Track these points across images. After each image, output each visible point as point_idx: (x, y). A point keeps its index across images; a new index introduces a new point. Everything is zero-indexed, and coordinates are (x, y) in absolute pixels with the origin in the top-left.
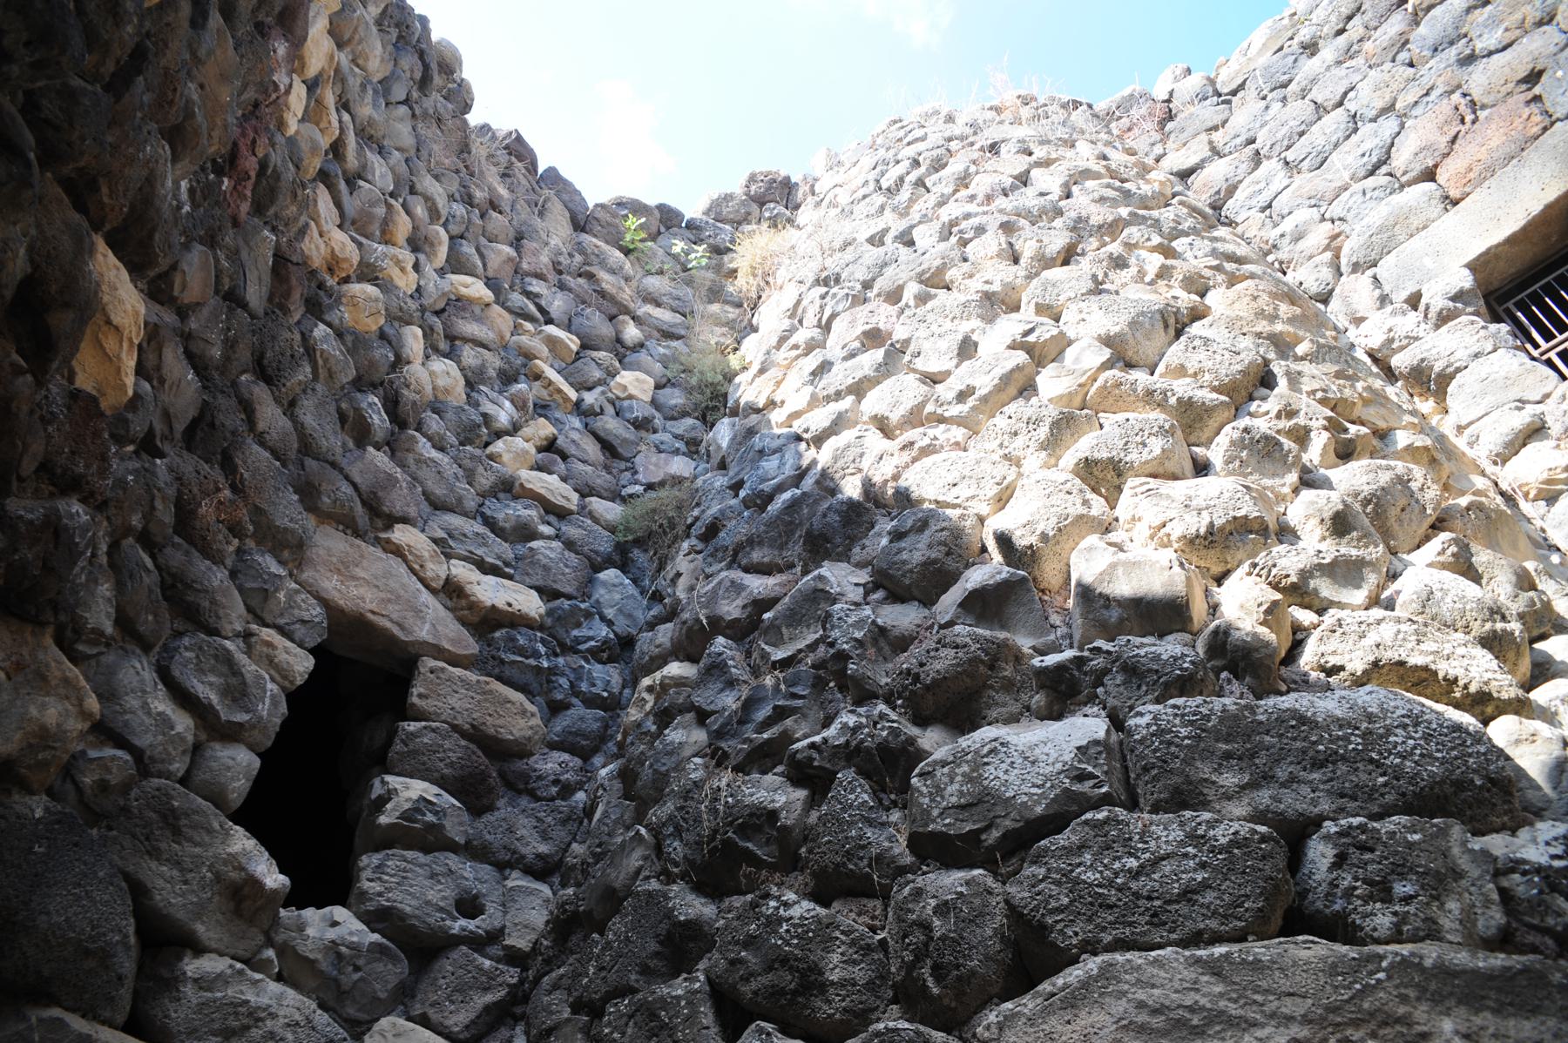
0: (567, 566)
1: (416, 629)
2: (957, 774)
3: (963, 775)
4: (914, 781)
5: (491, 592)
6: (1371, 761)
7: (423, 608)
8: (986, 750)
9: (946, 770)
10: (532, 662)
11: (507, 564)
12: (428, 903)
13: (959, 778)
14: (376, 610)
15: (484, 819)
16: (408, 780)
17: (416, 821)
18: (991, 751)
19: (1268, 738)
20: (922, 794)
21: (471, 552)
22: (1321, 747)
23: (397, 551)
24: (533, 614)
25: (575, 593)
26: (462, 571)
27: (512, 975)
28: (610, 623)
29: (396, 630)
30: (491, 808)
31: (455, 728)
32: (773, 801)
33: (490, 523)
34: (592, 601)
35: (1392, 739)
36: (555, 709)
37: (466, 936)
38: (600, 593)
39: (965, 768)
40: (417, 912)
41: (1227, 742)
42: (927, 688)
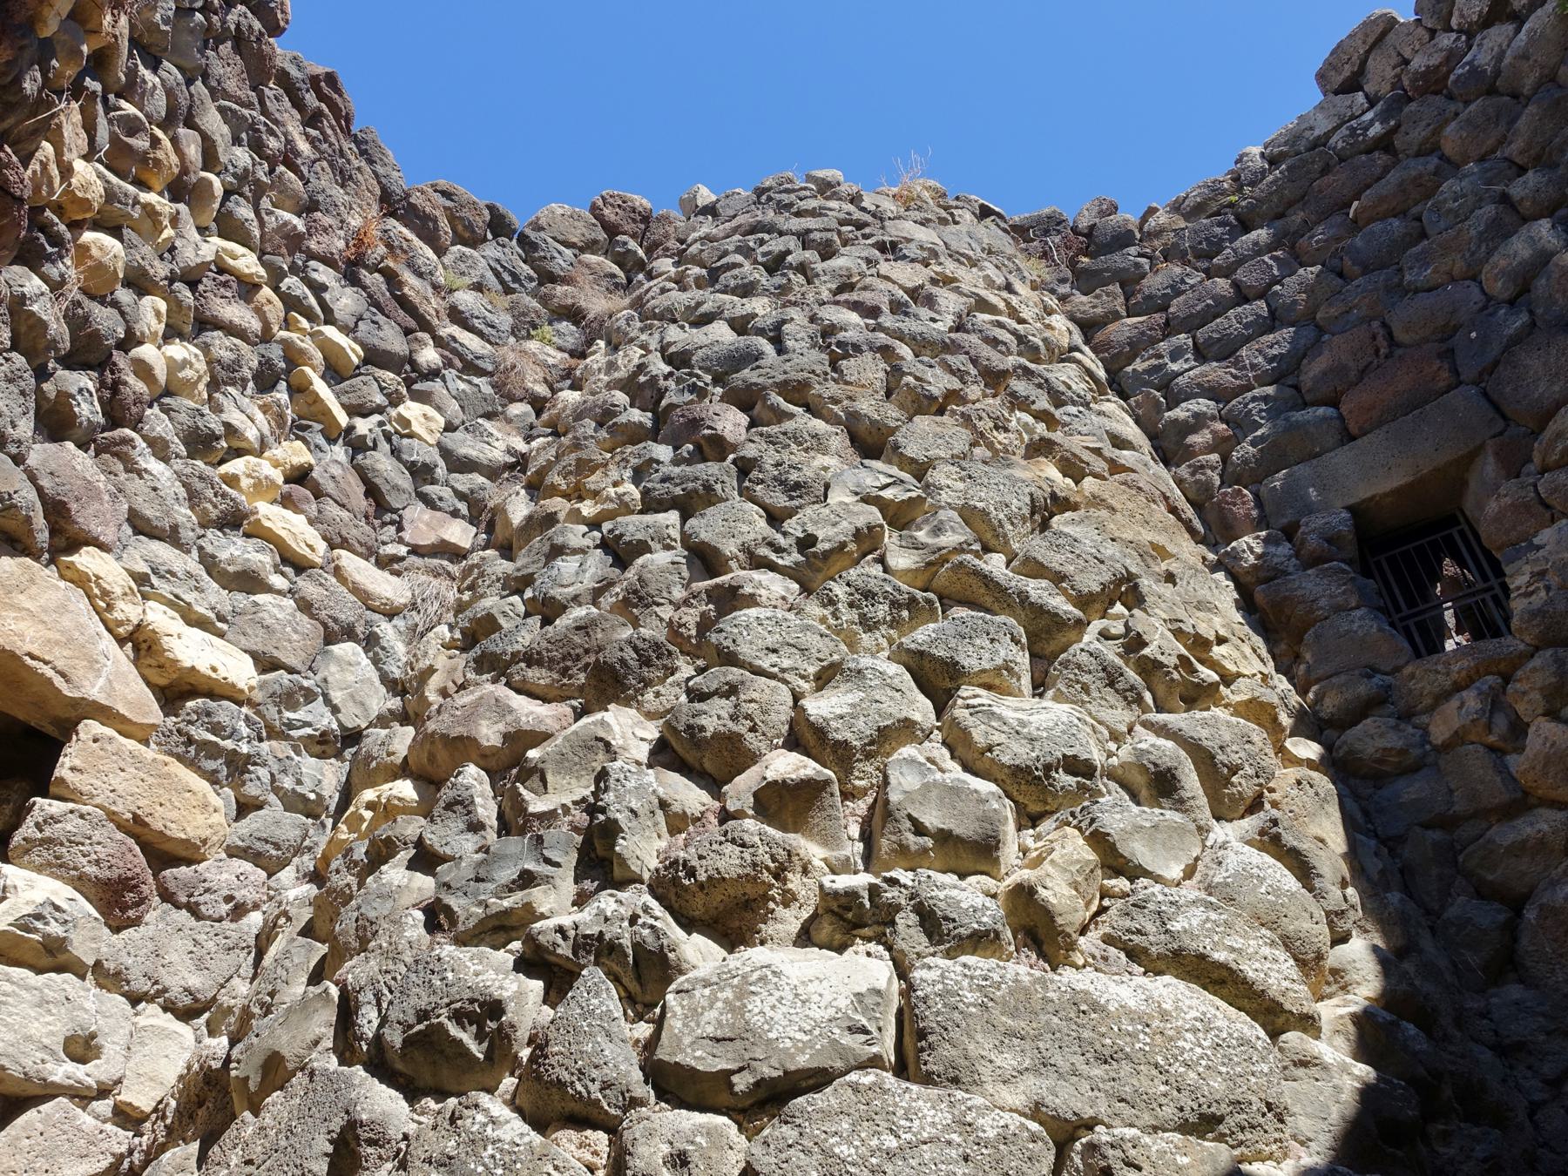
0: (296, 631)
1: (86, 683)
2: (717, 999)
3: (726, 1001)
4: (670, 997)
6: (1156, 1066)
7: (102, 659)
8: (755, 976)
9: (707, 992)
10: (228, 744)
11: (221, 618)
12: (28, 1038)
13: (720, 1004)
14: (37, 653)
15: (125, 934)
16: (34, 875)
17: (36, 930)
18: (760, 979)
19: (1056, 1020)
20: (675, 1015)
21: (176, 596)
22: (1108, 1041)
23: (81, 581)
24: (242, 685)
25: (299, 667)
26: (160, 618)
27: (120, 1139)
28: (335, 710)
29: (59, 682)
30: (136, 922)
31: (112, 816)
32: (501, 988)
33: (209, 563)
34: (318, 678)
35: (1181, 1043)
36: (245, 808)
37: (71, 1087)
38: (332, 671)
39: (728, 994)
40: (11, 1049)
41: (1013, 1016)
42: (701, 886)
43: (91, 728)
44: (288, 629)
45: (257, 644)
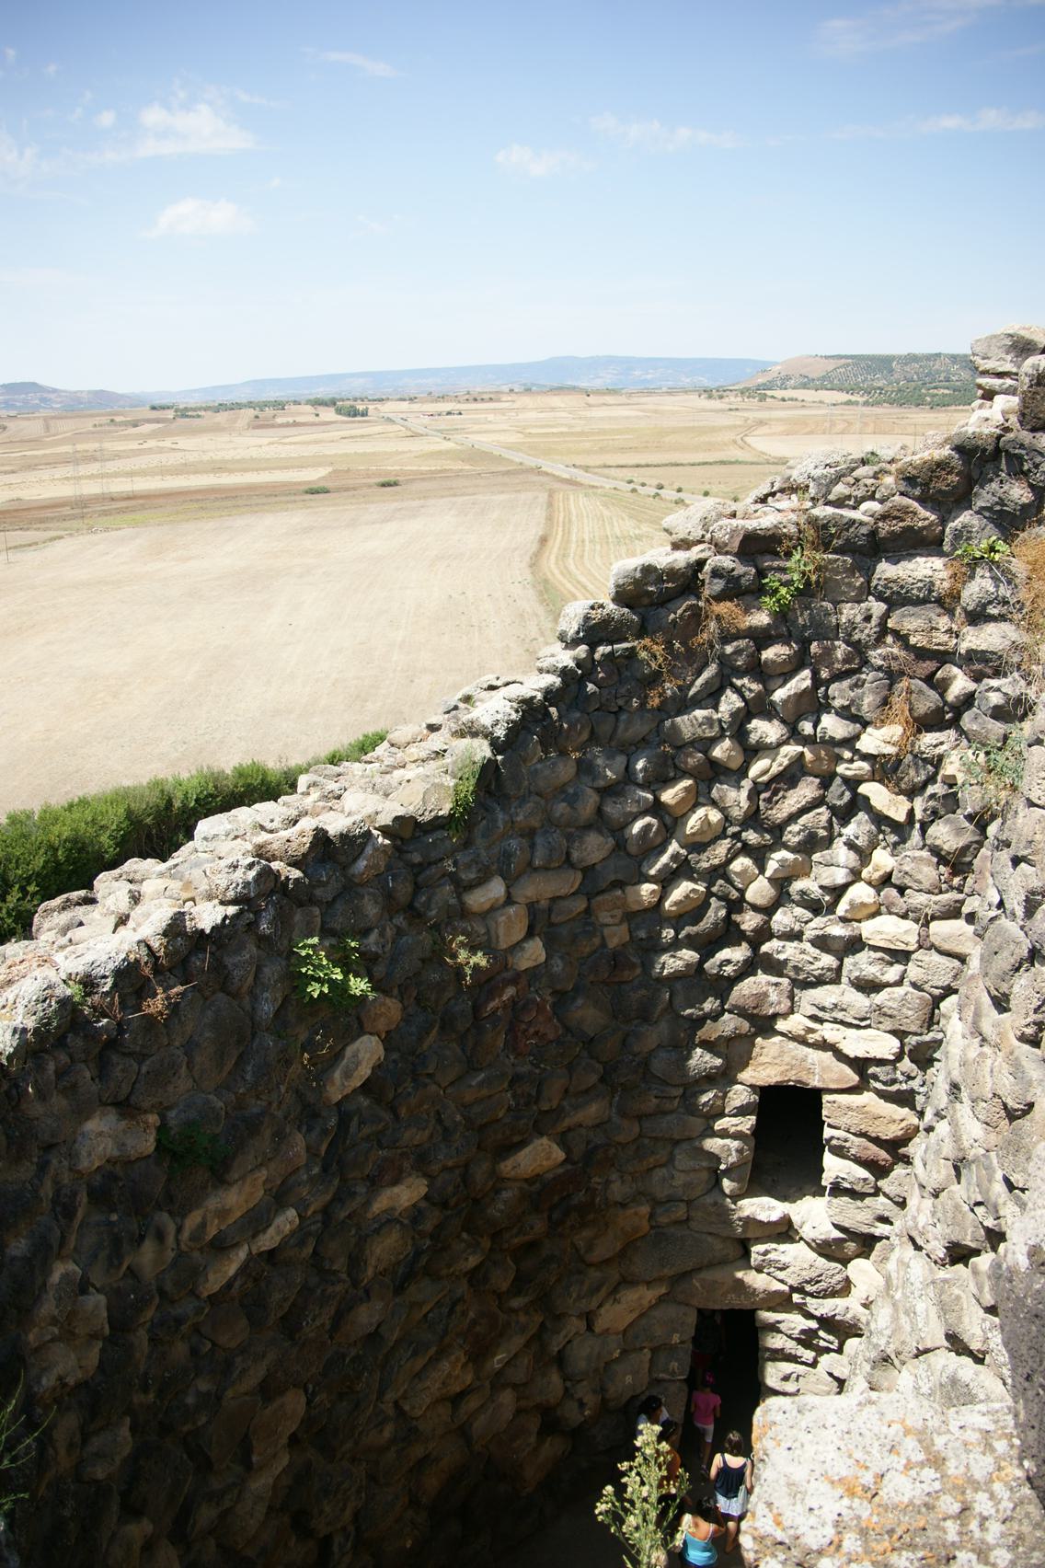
0: (909, 1009)
5: (857, 1043)
26: (829, 1032)
43: (826, 1098)
44: (904, 1010)
45: (888, 1024)
